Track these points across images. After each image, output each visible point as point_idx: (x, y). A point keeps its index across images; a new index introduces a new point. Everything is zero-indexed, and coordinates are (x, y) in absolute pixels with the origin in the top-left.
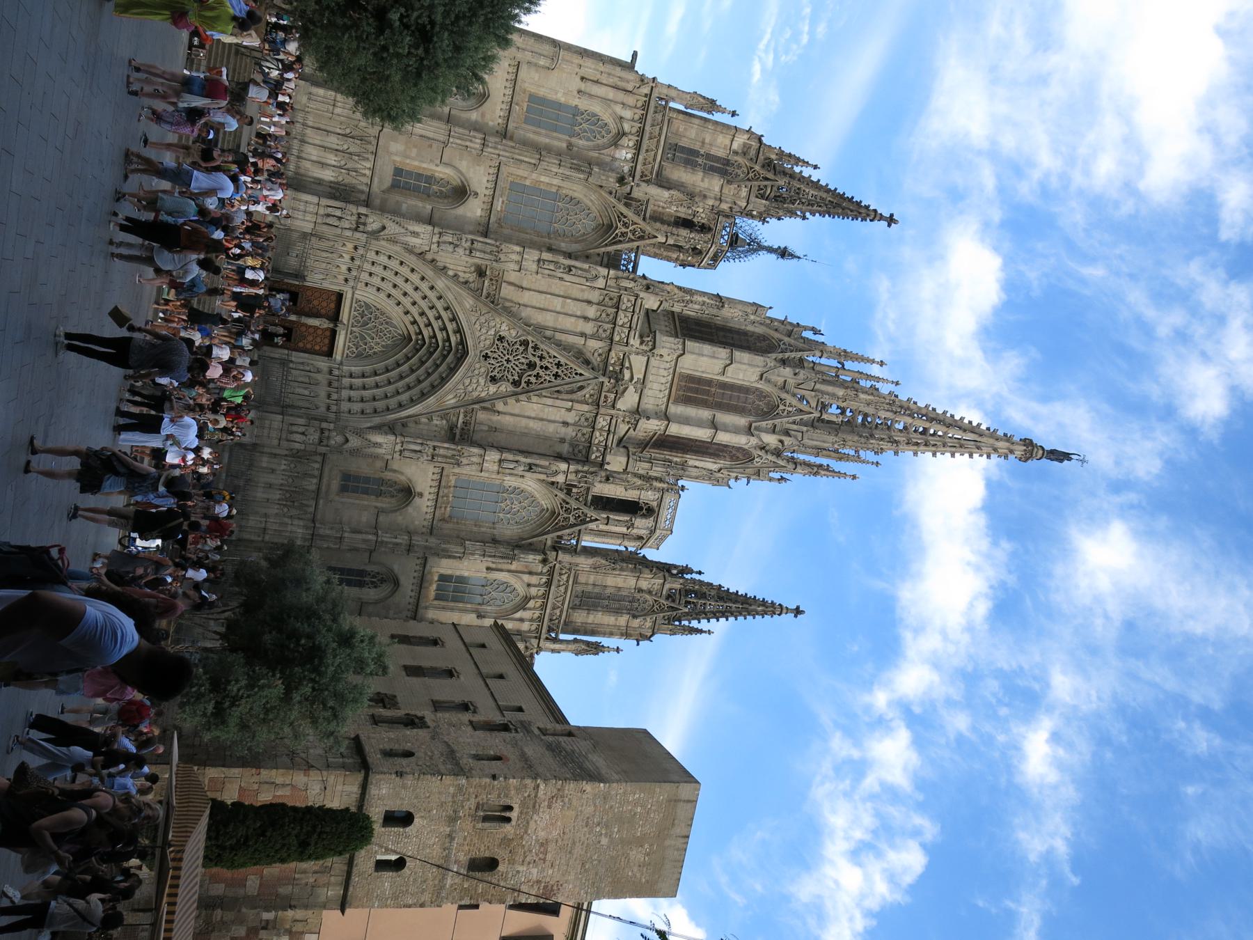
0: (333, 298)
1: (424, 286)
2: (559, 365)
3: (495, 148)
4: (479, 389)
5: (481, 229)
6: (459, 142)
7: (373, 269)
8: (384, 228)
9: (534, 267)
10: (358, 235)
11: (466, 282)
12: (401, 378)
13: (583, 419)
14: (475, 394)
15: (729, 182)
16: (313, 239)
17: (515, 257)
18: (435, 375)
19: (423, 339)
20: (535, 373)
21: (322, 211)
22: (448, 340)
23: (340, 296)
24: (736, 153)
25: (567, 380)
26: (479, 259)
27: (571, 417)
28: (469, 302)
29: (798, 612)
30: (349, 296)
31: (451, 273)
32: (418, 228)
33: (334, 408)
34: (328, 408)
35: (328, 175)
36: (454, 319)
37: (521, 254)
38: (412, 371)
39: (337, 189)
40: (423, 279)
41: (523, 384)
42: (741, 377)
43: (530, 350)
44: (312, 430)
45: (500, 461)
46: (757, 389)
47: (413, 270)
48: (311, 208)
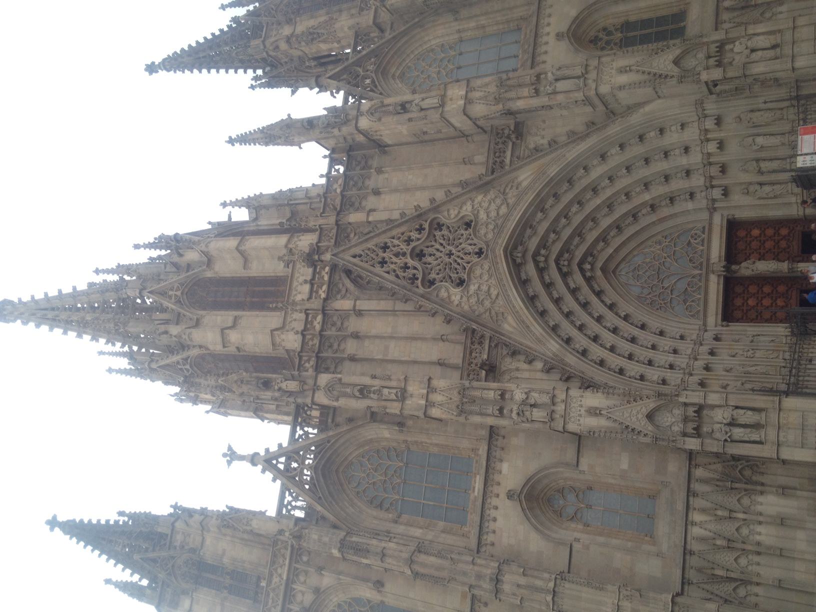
0: (738, 314)
1: (581, 341)
2: (383, 263)
3: (479, 577)
4: (485, 205)
5: (500, 442)
6: (539, 583)
7: (671, 358)
8: (650, 416)
9: (410, 389)
10: (695, 397)
11: (514, 353)
12: (610, 206)
13: (357, 204)
14: (492, 194)
15: (193, 551)
16: (783, 387)
17: (437, 398)
18: (553, 214)
19: (582, 271)
20: (413, 244)
21: (772, 434)
22: (541, 271)
23: (728, 315)
24: (184, 592)
25: (370, 245)
26: (490, 391)
27: (371, 202)
28: (509, 326)
29: (151, 69)
30: (711, 320)
31: (539, 365)
32: (592, 422)
33: (709, 124)
34: (719, 121)
35: (770, 504)
36: (531, 300)
37: (429, 404)
38: (592, 218)
39: (749, 481)
40: (584, 353)
41: (426, 226)
42: (219, 318)
43: (420, 276)
44: (739, 60)
45: (442, 105)
46: (204, 309)
47: (602, 363)
48: (791, 436)
